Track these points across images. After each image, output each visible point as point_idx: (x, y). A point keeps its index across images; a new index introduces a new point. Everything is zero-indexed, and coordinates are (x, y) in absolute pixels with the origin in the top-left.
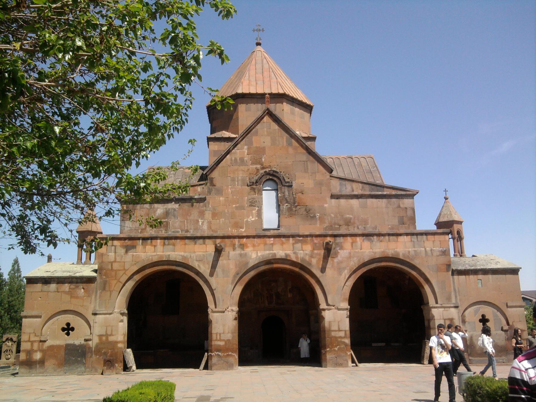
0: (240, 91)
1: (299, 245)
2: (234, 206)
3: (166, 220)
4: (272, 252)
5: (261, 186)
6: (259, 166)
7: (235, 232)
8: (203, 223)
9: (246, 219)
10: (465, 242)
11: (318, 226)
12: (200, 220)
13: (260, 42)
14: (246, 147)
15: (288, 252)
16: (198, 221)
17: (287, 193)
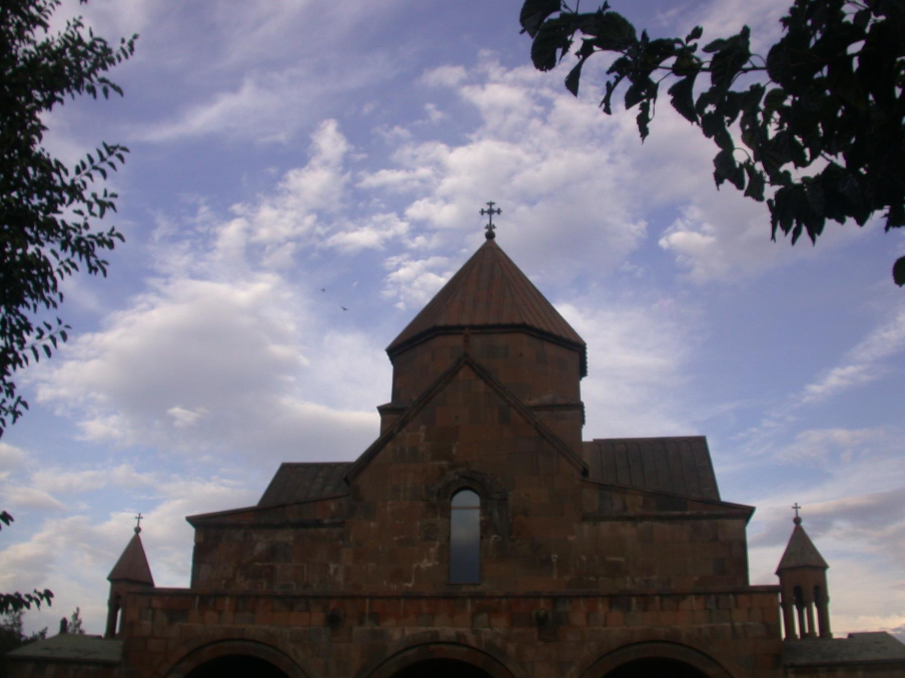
0: (441, 322)
1: (483, 617)
2: (395, 538)
3: (271, 563)
4: (430, 629)
5: (448, 500)
6: (444, 463)
7: (394, 587)
8: (336, 571)
9: (415, 565)
10: (831, 607)
11: (555, 577)
12: (332, 566)
13: (494, 230)
14: (423, 427)
15: (463, 630)
16: (327, 566)
17: (496, 514)
